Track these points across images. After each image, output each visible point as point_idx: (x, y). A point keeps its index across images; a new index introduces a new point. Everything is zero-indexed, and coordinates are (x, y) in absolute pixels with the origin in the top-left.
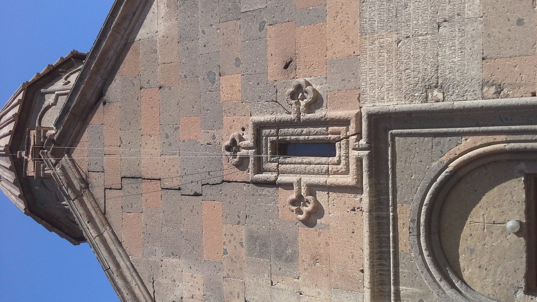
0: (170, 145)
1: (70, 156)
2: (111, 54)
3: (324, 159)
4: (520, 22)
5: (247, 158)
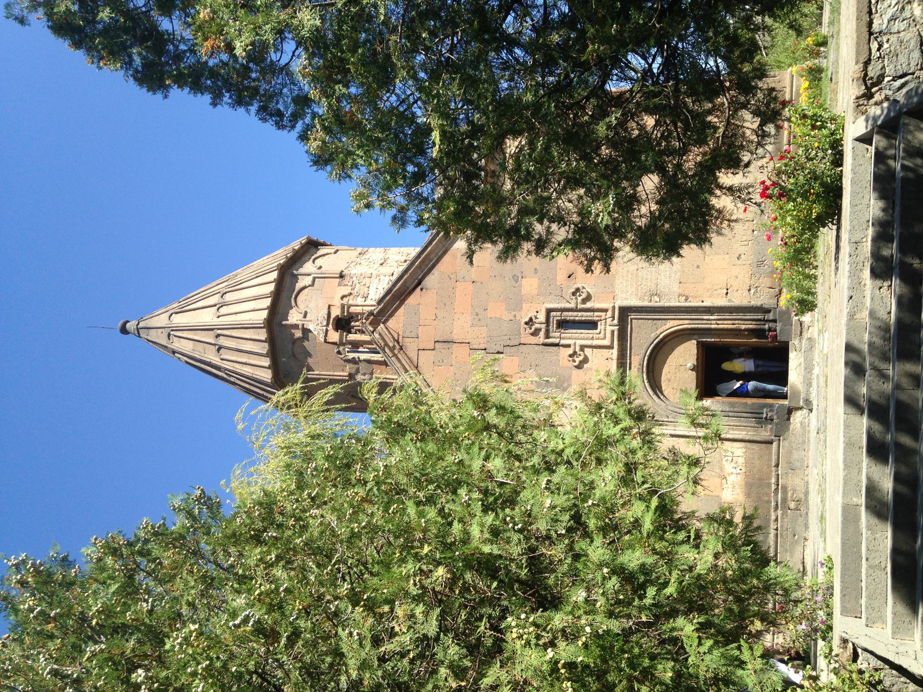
0: (479, 320)
2: (432, 257)
3: (590, 331)
4: (698, 267)
5: (540, 330)
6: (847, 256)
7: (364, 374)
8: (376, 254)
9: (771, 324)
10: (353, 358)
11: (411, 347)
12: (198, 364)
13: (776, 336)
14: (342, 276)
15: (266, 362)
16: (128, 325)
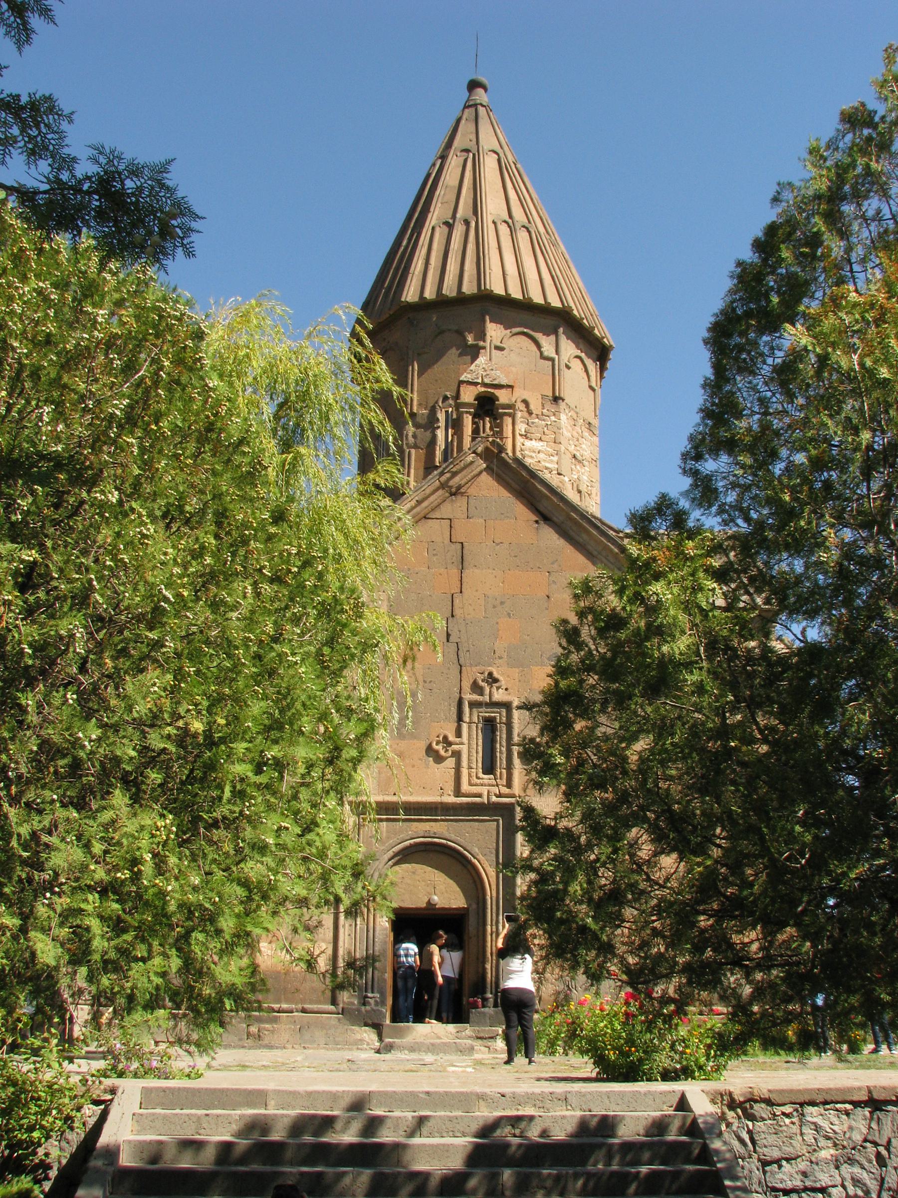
0: (494, 607)
1: (485, 469)
2: (585, 536)
3: (480, 765)
6: (551, 1090)
7: (414, 436)
8: (589, 447)
9: (491, 1000)
10: (438, 420)
11: (455, 508)
12: (426, 193)
13: (475, 1006)
14: (556, 399)
15: (430, 293)
16: (480, 91)
